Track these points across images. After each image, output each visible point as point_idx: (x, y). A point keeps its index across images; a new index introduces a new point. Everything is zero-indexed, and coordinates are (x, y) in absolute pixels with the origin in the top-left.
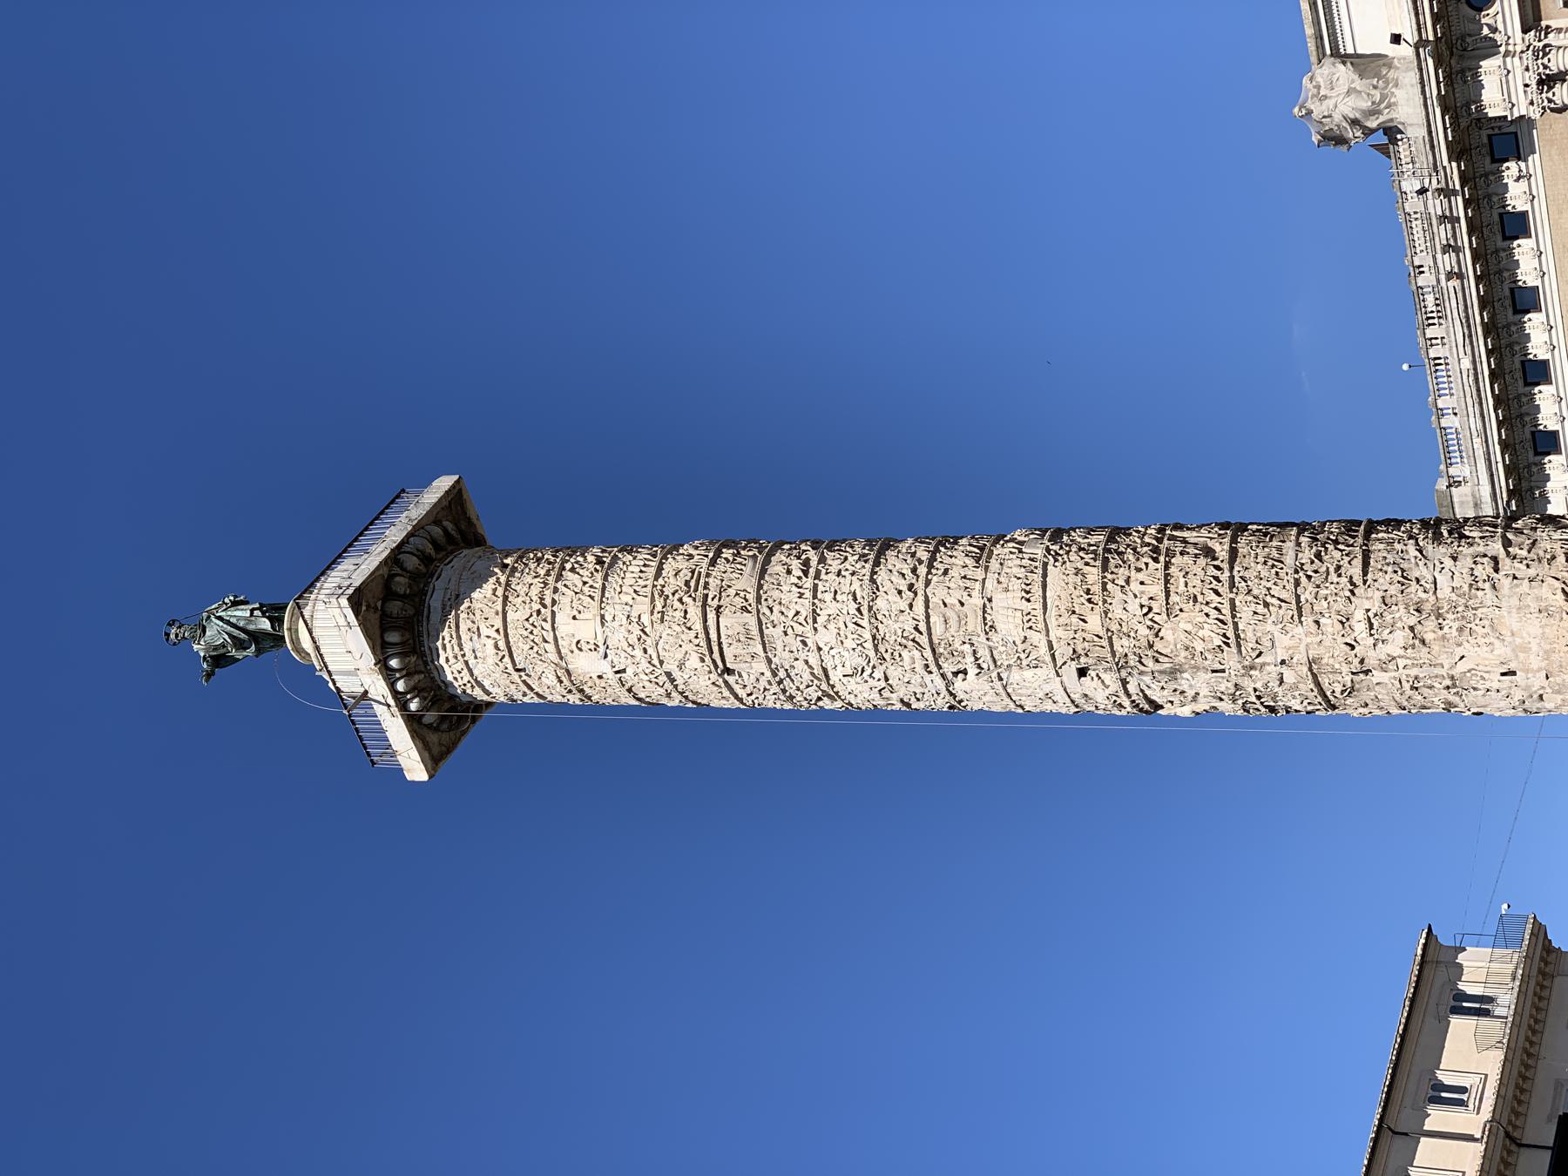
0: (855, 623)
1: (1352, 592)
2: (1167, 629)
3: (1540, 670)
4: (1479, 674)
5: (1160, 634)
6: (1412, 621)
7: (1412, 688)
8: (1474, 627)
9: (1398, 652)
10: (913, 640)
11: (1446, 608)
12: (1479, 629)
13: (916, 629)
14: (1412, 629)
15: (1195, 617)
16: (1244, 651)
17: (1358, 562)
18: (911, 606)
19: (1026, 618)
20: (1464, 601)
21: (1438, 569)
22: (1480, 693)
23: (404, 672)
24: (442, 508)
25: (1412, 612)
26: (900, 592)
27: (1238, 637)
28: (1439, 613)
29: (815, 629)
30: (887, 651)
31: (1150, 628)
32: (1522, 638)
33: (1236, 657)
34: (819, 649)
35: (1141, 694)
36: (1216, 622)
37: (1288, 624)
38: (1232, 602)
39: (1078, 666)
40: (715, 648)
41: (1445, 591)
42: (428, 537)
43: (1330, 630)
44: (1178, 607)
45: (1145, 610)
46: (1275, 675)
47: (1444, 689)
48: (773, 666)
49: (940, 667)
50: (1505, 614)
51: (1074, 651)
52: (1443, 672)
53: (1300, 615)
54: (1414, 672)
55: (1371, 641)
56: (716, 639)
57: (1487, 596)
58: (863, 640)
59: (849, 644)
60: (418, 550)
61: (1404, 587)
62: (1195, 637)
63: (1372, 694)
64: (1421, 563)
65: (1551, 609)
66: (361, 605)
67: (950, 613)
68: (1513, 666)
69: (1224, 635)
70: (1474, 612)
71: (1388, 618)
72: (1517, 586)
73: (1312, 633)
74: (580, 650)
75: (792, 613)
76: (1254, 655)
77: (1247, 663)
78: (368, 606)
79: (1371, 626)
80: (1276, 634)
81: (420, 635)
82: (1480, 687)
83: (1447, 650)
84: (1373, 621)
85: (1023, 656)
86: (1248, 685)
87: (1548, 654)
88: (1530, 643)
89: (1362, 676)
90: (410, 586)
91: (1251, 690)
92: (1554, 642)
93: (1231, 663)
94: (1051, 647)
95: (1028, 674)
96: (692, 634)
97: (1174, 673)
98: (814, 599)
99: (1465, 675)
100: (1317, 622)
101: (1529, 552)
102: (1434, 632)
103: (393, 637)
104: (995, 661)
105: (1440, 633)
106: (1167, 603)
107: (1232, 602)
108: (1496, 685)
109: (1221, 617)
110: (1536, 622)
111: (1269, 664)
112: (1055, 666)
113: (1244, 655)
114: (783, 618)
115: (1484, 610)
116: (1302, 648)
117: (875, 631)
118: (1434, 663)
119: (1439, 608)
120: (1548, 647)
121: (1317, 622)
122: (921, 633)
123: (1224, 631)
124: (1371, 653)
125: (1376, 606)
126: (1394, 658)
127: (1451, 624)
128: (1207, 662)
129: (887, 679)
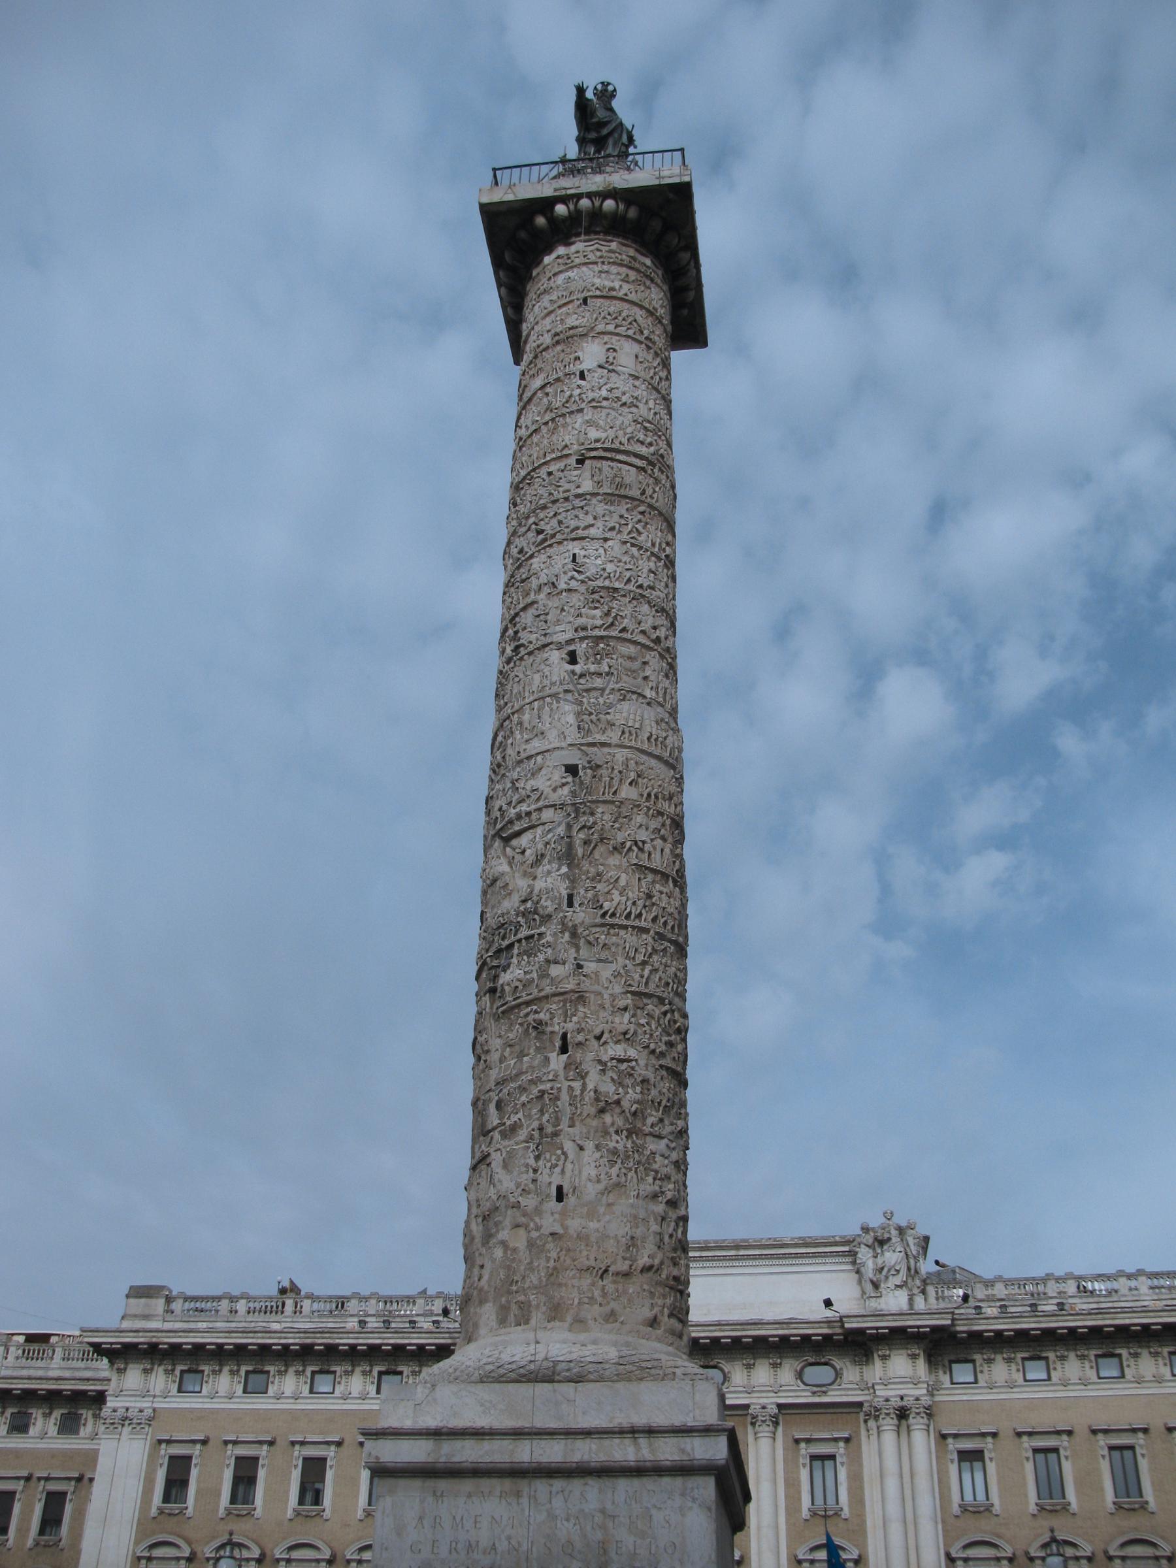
1: (653, 1052)
2: (620, 861)
3: (566, 1228)
4: (561, 1163)
5: (616, 853)
6: (625, 1104)
7: (543, 1092)
10: (612, 624)
11: (638, 1142)
12: (614, 1171)
14: (618, 1102)
15: (633, 893)
16: (594, 930)
18: (643, 632)
19: (633, 731)
20: (643, 1160)
22: (532, 1162)
25: (635, 1106)
27: (612, 926)
29: (625, 543)
30: (601, 597)
31: (623, 843)
32: (604, 1214)
33: (588, 921)
34: (606, 540)
35: (539, 822)
36: (628, 910)
37: (624, 979)
39: (580, 766)
40: (608, 455)
41: (652, 1145)
43: (617, 1020)
44: (642, 877)
46: (562, 956)
47: (541, 1124)
48: (588, 497)
49: (582, 639)
50: (631, 1201)
51: (598, 766)
52: (564, 1125)
53: (633, 993)
54: (565, 1097)
55: (605, 1058)
56: (617, 457)
57: (648, 1186)
58: (613, 580)
59: (610, 568)
61: (656, 1104)
62: (611, 886)
63: (532, 1051)
65: (634, 1250)
67: (636, 665)
68: (571, 1200)
69: (613, 915)
71: (629, 1081)
72: (656, 1220)
73: (614, 1001)
74: (608, 350)
76: (591, 938)
77: (580, 930)
79: (621, 1061)
80: (613, 967)
81: (625, 237)
82: (541, 1163)
83: (592, 1134)
84: (625, 1065)
85: (593, 717)
86: (549, 931)
87: (582, 1237)
88: (599, 1221)
89: (558, 1043)
91: (543, 929)
92: (599, 1247)
93: (583, 915)
94: (603, 745)
95: (571, 719)
96: (625, 441)
97: (568, 856)
98: (651, 552)
99: (559, 1148)
100: (625, 1009)
102: (613, 1124)
103: (633, 213)
104: (588, 691)
105: (612, 1130)
106: (647, 868)
108: (544, 1178)
109: (633, 916)
110: (621, 1233)
111: (578, 951)
112: (582, 745)
113: (590, 929)
115: (635, 1180)
116: (596, 988)
117: (622, 593)
118: (575, 1118)
119: (637, 1135)
120: (593, 1239)
121: (625, 1009)
122: (620, 632)
123: (618, 915)
124: (590, 1056)
125: (641, 1071)
127: (619, 1142)
128: (582, 891)
129: (570, 590)
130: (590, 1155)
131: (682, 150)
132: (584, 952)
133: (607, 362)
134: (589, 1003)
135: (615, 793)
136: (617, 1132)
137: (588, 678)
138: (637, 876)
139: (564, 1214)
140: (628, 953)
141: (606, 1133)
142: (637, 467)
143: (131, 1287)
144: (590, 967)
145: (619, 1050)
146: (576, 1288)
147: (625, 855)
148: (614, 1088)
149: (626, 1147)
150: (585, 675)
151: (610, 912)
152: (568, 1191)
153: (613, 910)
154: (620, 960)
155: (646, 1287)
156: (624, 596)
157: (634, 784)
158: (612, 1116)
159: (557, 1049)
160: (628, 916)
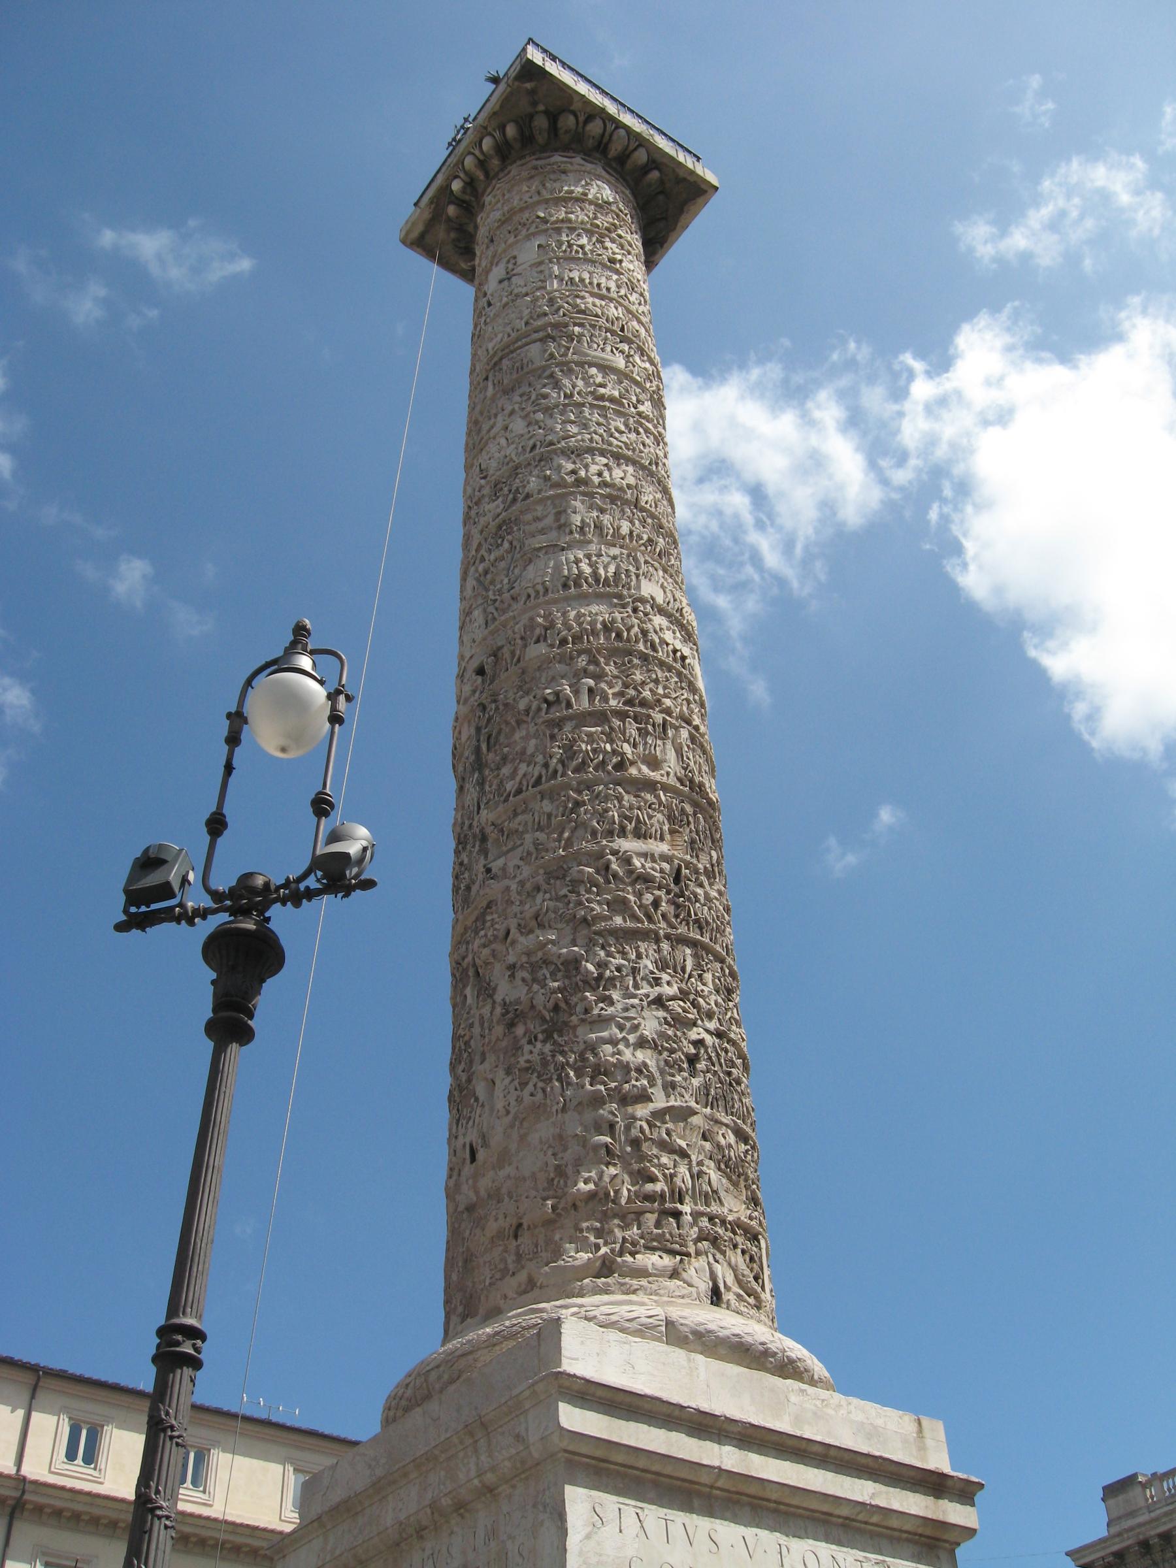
0: (534, 447)
8: (530, 1087)
9: (498, 997)
11: (560, 1039)
13: (528, 496)
23: (481, 157)
24: (674, 171)
26: (574, 472)
29: (527, 415)
40: (507, 351)
42: (631, 148)
45: (551, 698)
55: (511, 959)
56: (516, 345)
60: (611, 135)
64: (636, 1001)
66: (531, 80)
68: (481, 1155)
70: (555, 1077)
74: (508, 262)
75: (546, 390)
78: (533, 92)
90: (566, 132)
103: (511, 131)
105: (524, 1041)
109: (544, 779)
111: (486, 857)
114: (539, 386)
123: (524, 788)
126: (491, 996)
130: (502, 1080)
131: (531, 40)
132: (493, 852)
133: (507, 273)
134: (496, 905)
135: (519, 660)
136: (530, 1042)
137: (492, 569)
138: (548, 733)
139: (475, 1177)
140: (539, 823)
141: (517, 1048)
142: (541, 340)
143: (1104, 1488)
144: (496, 866)
145: (525, 942)
146: (487, 1265)
147: (533, 718)
148: (527, 988)
149: (543, 1054)
150: (489, 568)
151: (513, 791)
152: (477, 1143)
153: (516, 786)
154: (528, 838)
156: (529, 464)
157: (542, 639)
158: (525, 1024)
159: (471, 979)
160: (538, 781)
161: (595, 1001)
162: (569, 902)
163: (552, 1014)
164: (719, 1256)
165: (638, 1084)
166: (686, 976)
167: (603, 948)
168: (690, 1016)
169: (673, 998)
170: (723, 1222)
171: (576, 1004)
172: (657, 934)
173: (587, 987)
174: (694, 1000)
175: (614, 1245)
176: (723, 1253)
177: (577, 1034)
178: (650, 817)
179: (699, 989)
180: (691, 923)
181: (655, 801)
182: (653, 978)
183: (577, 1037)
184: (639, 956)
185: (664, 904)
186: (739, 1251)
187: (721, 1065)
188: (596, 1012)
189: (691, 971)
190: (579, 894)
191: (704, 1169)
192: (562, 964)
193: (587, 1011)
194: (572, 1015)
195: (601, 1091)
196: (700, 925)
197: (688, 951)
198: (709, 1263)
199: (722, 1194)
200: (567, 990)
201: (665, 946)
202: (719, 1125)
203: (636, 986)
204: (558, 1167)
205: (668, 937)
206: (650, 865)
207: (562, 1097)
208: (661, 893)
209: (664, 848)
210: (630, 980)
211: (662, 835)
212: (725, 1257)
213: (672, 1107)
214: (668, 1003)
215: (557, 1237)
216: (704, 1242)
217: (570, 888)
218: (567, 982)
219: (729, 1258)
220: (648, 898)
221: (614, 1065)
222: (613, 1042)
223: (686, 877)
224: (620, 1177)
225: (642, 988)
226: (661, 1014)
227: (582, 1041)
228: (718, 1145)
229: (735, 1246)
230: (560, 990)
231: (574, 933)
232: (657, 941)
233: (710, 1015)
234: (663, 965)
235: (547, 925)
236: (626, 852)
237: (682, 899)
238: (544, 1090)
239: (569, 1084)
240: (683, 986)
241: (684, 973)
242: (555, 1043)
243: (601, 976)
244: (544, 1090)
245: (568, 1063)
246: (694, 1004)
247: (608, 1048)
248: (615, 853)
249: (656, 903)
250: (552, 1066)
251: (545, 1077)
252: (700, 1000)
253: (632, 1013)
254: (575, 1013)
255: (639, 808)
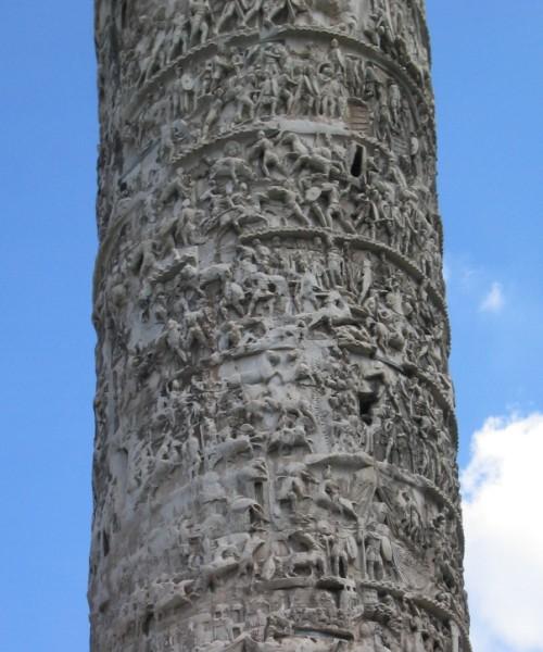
11: (199, 385)
17: (291, 226)
20: (212, 409)
21: (274, 353)
28: (189, 377)
38: (211, 50)
41: (229, 374)
64: (292, 328)
70: (192, 431)
101: (322, 504)
107: (211, 50)
149: (178, 405)
155: (221, 607)
161: (241, 330)
162: (212, 206)
163: (189, 354)
164: (389, 639)
165: (291, 430)
166: (363, 294)
167: (254, 261)
168: (364, 344)
169: (343, 322)
170: (399, 598)
171: (219, 338)
172: (324, 238)
173: (233, 315)
174: (373, 325)
175: (256, 629)
176: (397, 635)
177: (219, 375)
178: (322, 84)
179: (380, 311)
180: (374, 227)
181: (328, 62)
182: (317, 297)
183: (218, 379)
184: (300, 269)
185: (335, 200)
186: (418, 636)
187: (407, 409)
188: (242, 343)
189: (370, 288)
190: (225, 194)
191: (375, 534)
192: (203, 288)
193: (231, 343)
194: (213, 352)
195: (245, 443)
196: (386, 229)
197: (367, 263)
198: (375, 646)
199: (399, 567)
200: (207, 320)
201: (335, 258)
202: (399, 483)
203: (296, 308)
204: (193, 541)
205: (339, 243)
206: (319, 149)
207: (200, 454)
208: (333, 186)
209: (339, 126)
210: (286, 301)
211: (337, 108)
212: (399, 641)
213: (335, 458)
214: (335, 329)
215: (191, 626)
216: (370, 623)
217: (214, 187)
218: (208, 310)
219: (405, 642)
220: (314, 193)
221: (264, 409)
222: (264, 381)
223: (369, 165)
224: (266, 548)
225: (303, 310)
226: (330, 342)
227: (225, 383)
228: (396, 507)
229: (414, 629)
230: (200, 321)
231: (218, 248)
232: (327, 248)
233: (395, 346)
234: (331, 280)
235: (185, 240)
236: (286, 132)
237: (362, 195)
238: (178, 448)
239: (207, 438)
240: (358, 307)
241: (361, 290)
242: (195, 390)
243: (249, 296)
244: (178, 448)
245: (207, 413)
246: (371, 329)
247: (258, 389)
248: (272, 134)
249: (325, 198)
250: (189, 418)
251: (181, 433)
252: (381, 326)
253: (288, 342)
254: (218, 350)
255: (307, 73)
